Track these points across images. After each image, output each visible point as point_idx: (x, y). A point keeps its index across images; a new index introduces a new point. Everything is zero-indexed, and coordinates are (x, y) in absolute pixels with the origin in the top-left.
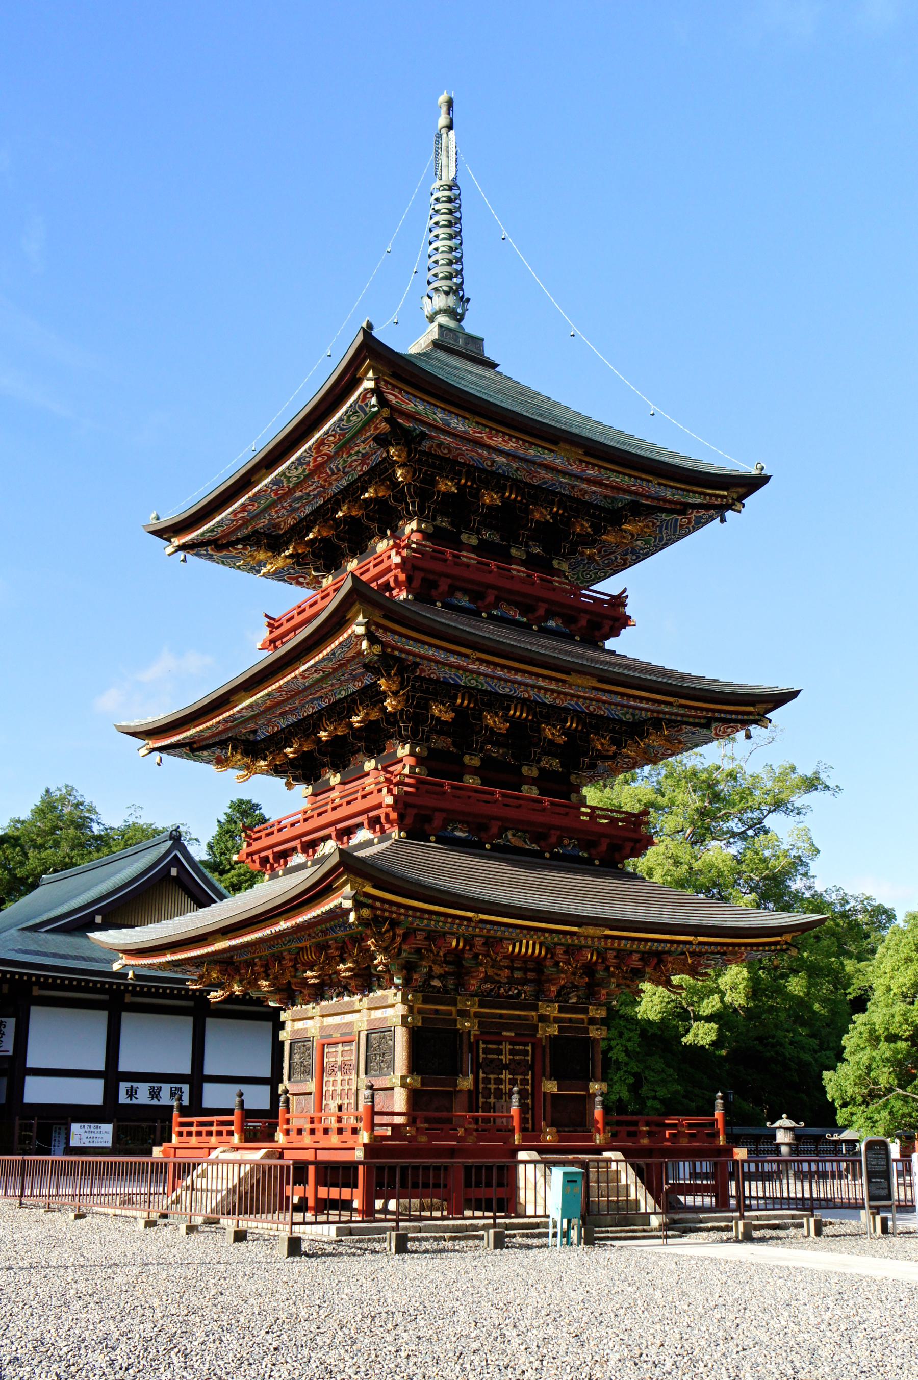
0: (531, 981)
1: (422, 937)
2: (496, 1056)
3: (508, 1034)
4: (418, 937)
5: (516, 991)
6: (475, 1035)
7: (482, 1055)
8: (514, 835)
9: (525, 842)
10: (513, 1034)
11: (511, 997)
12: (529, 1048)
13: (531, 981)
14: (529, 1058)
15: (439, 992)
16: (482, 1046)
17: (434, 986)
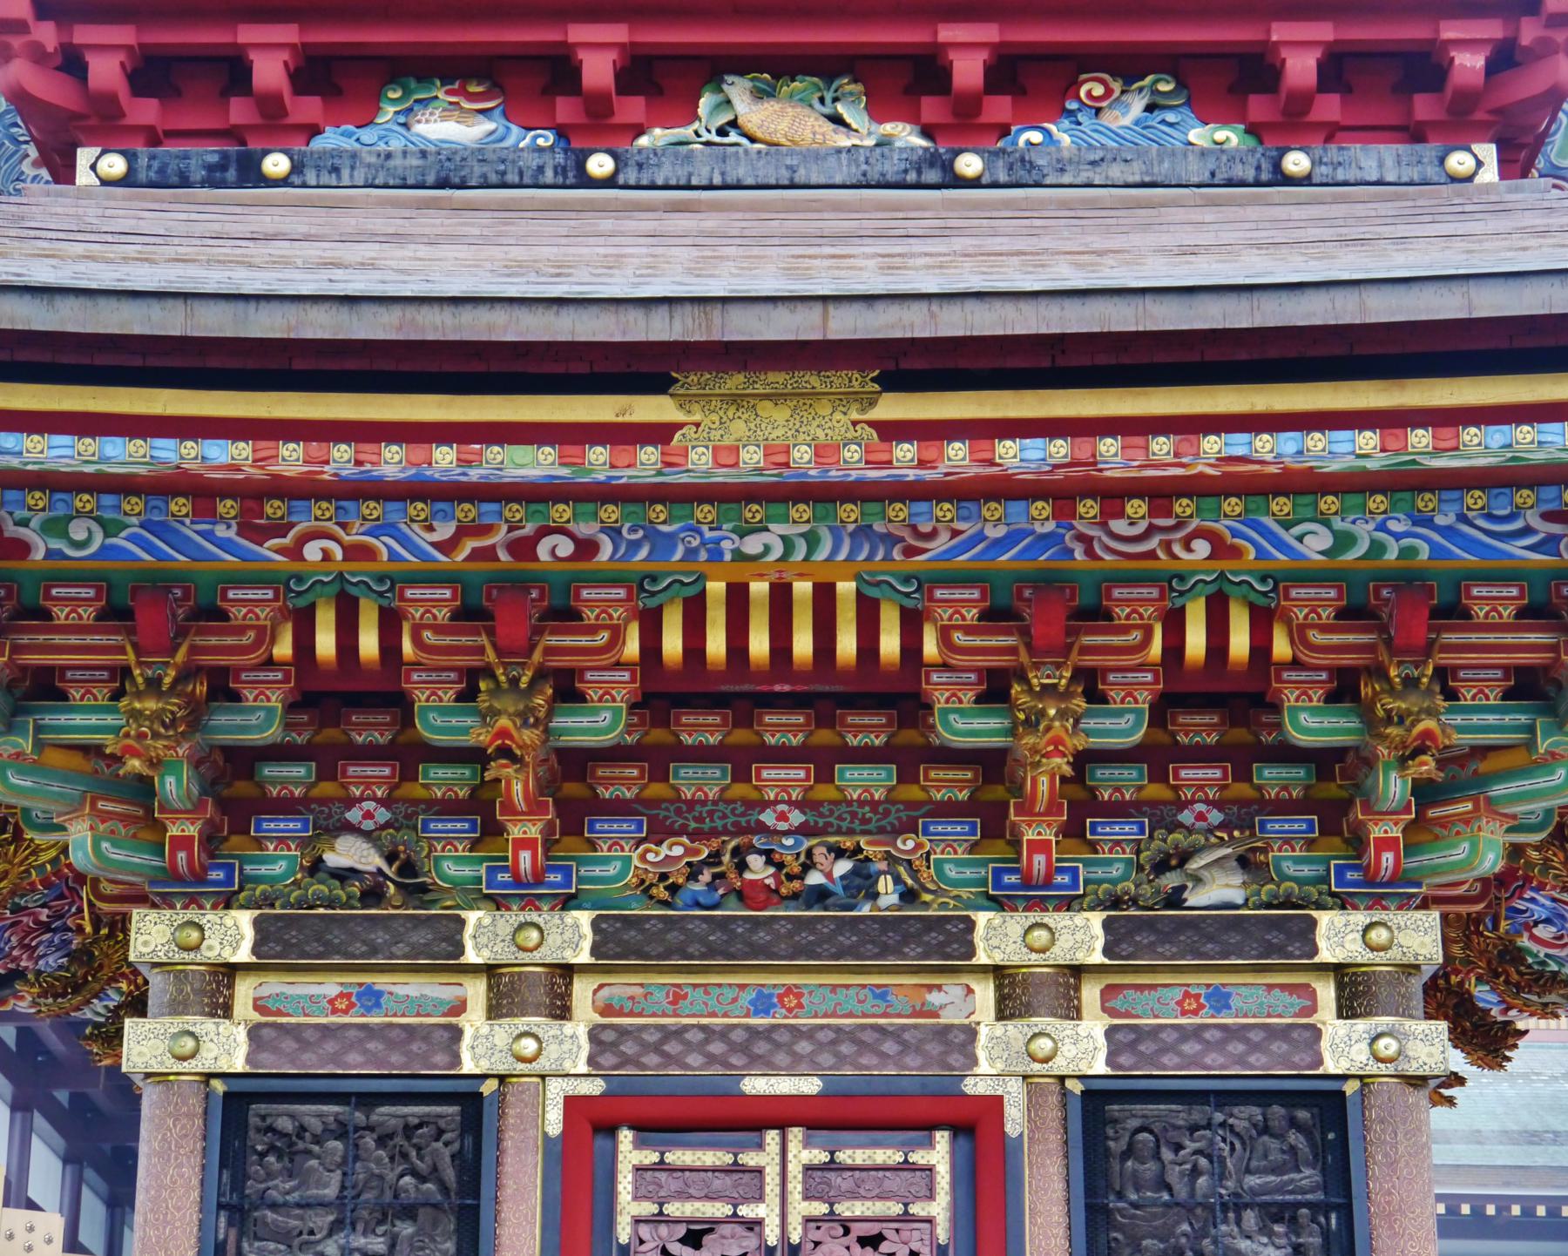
0: (948, 810)
1: (87, 614)
2: (721, 1210)
3: (784, 1086)
4: (61, 614)
5: (843, 867)
6: (572, 1104)
7: (629, 1206)
8: (760, 94)
9: (837, 120)
10: (810, 1086)
11: (820, 896)
12: (939, 1154)
13: (948, 810)
14: (939, 1208)
15: (373, 895)
16: (629, 1152)
17: (344, 875)
